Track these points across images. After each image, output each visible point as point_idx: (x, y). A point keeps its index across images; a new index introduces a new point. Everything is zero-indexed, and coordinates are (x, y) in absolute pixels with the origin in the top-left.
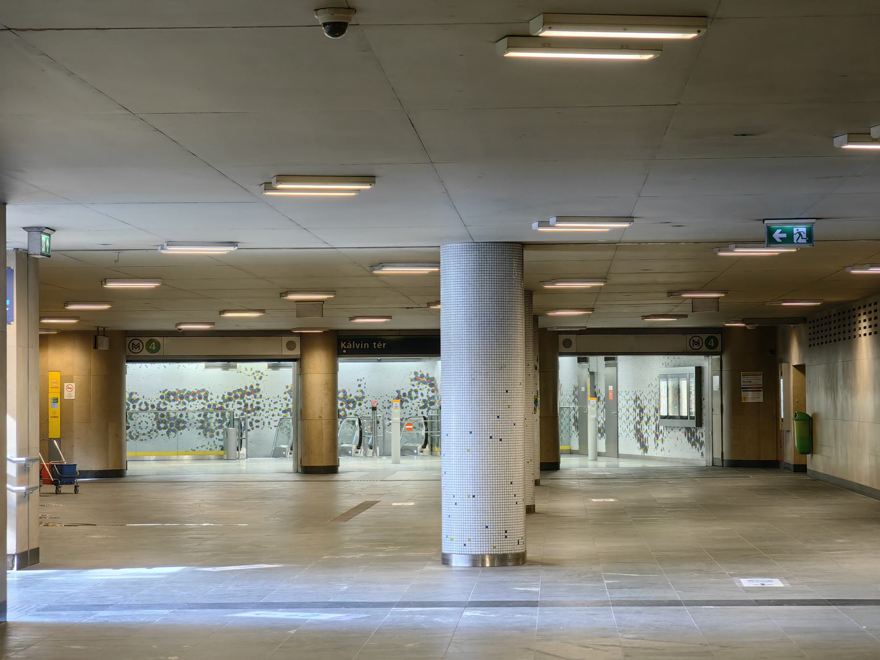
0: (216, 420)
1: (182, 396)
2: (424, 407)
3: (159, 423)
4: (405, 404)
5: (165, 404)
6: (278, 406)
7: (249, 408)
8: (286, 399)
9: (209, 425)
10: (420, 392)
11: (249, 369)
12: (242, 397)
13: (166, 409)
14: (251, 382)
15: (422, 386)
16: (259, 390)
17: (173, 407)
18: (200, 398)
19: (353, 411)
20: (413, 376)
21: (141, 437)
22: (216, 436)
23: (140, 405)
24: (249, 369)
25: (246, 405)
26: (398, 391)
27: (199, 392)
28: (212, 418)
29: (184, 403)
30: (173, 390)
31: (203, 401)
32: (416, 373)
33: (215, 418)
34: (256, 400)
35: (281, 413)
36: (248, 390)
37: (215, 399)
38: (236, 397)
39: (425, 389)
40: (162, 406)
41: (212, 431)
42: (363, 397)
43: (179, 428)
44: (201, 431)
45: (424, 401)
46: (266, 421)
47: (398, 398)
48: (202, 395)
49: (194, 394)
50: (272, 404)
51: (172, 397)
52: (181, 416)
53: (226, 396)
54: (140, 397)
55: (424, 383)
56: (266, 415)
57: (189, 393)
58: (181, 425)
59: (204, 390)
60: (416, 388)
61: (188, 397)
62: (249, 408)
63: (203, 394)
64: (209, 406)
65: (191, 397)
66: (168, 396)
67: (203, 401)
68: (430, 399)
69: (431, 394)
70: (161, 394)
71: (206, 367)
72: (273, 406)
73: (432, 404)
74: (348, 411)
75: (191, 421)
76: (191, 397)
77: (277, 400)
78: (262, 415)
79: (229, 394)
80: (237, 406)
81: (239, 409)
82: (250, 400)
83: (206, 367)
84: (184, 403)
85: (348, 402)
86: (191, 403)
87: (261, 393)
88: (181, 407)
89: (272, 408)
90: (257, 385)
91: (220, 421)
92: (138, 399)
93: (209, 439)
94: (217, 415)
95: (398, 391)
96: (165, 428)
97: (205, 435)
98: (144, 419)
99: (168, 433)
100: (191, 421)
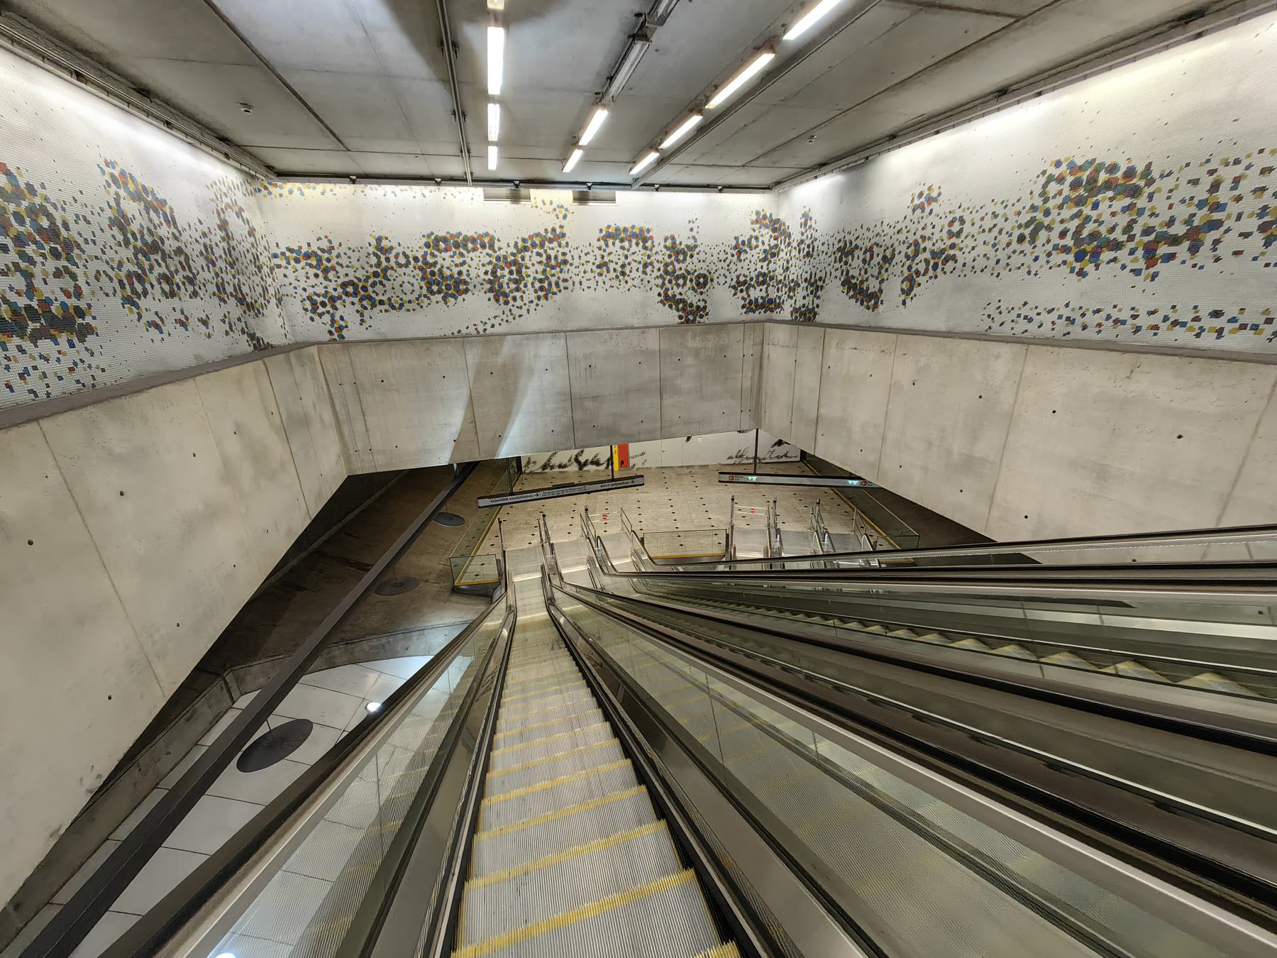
0: (510, 280)
1: (458, 243)
2: (764, 260)
3: (429, 284)
4: (743, 257)
5: (433, 255)
6: (591, 258)
7: (553, 262)
8: (600, 248)
9: (501, 286)
10: (761, 239)
11: (548, 203)
12: (542, 245)
13: (436, 263)
14: (550, 222)
15: (764, 231)
16: (563, 235)
17: (446, 261)
18: (483, 246)
19: (683, 266)
20: (754, 217)
21: (407, 306)
22: (512, 302)
23: (397, 256)
24: (548, 203)
25: (549, 258)
26: (736, 238)
27: (481, 236)
28: (503, 276)
29: (462, 255)
30: (442, 234)
31: (487, 250)
32: (758, 213)
33: (508, 276)
34: (561, 250)
35: (594, 268)
36: (549, 235)
37: (505, 247)
38: (534, 245)
39: (766, 235)
40: (430, 260)
41: (506, 295)
42: (696, 246)
43: (460, 292)
44: (491, 295)
45: (765, 251)
46: (577, 280)
47: (736, 247)
48: (485, 242)
49: (473, 240)
50: (583, 255)
51: (442, 245)
52: (460, 273)
53: (520, 244)
54: (395, 245)
55: (766, 227)
56: (576, 271)
57: (466, 239)
58: (462, 287)
59: (487, 234)
60: (756, 233)
61: (465, 246)
62: (553, 262)
63: (486, 240)
64: (498, 259)
65: (470, 246)
66: (435, 243)
67: (487, 250)
68: (771, 248)
69: (773, 242)
70: (425, 240)
71: (487, 198)
72: (584, 259)
73: (773, 255)
74: (677, 266)
75: (475, 281)
76: (470, 246)
77: (589, 250)
78: (570, 272)
79: (524, 240)
80: (536, 259)
81: (540, 263)
82: (553, 250)
83: (487, 198)
84: (462, 255)
85: (678, 253)
86: (472, 254)
87: (566, 239)
88: (458, 260)
89: (583, 261)
90: (561, 227)
91: (516, 282)
92: (392, 248)
93: (506, 308)
94: (511, 273)
95: (736, 238)
96: (439, 292)
97: (497, 301)
98: (406, 279)
99: (444, 299)
100: (475, 281)
